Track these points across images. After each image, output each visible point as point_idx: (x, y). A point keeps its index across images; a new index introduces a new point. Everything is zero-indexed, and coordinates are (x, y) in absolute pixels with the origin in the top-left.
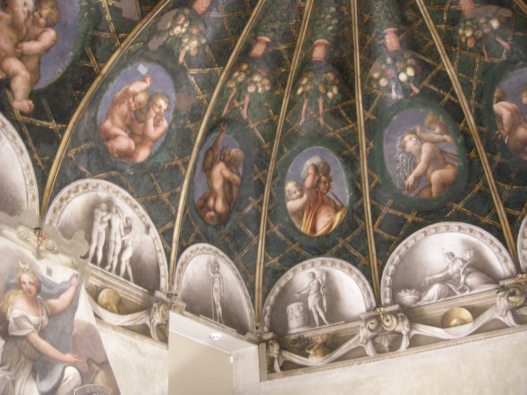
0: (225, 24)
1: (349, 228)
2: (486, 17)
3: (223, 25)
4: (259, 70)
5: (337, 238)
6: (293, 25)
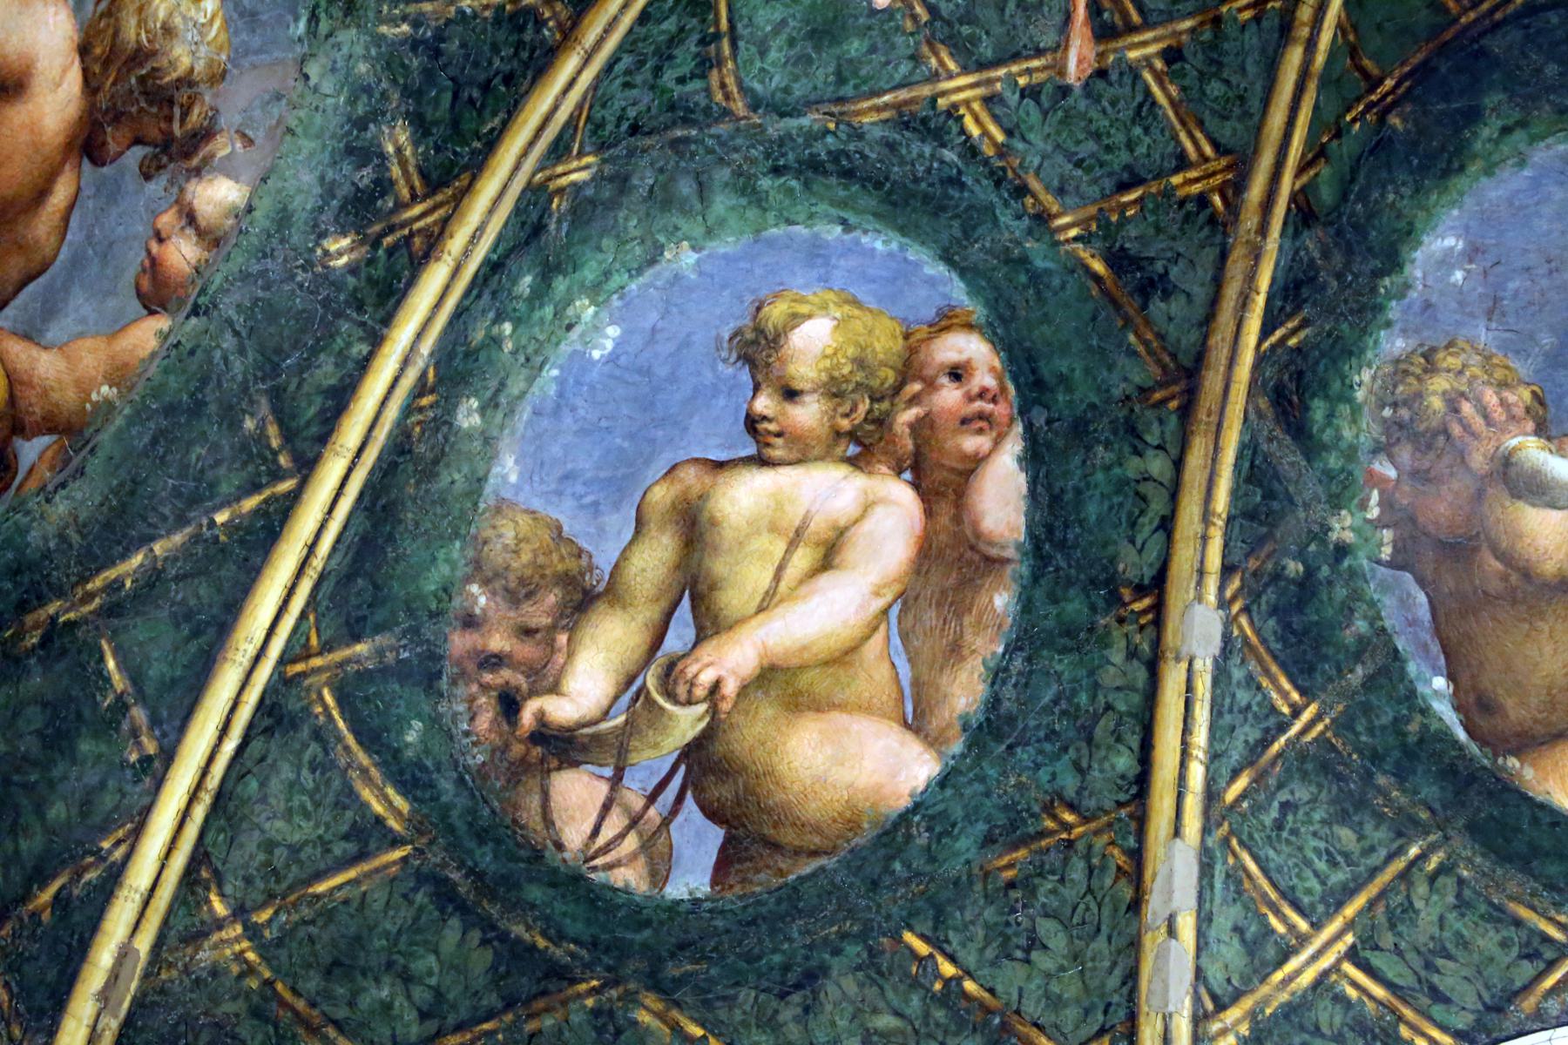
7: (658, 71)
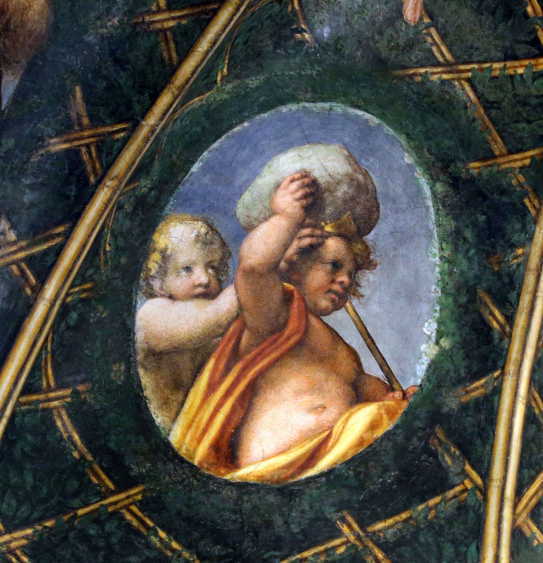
1: (399, 481)
5: (330, 512)
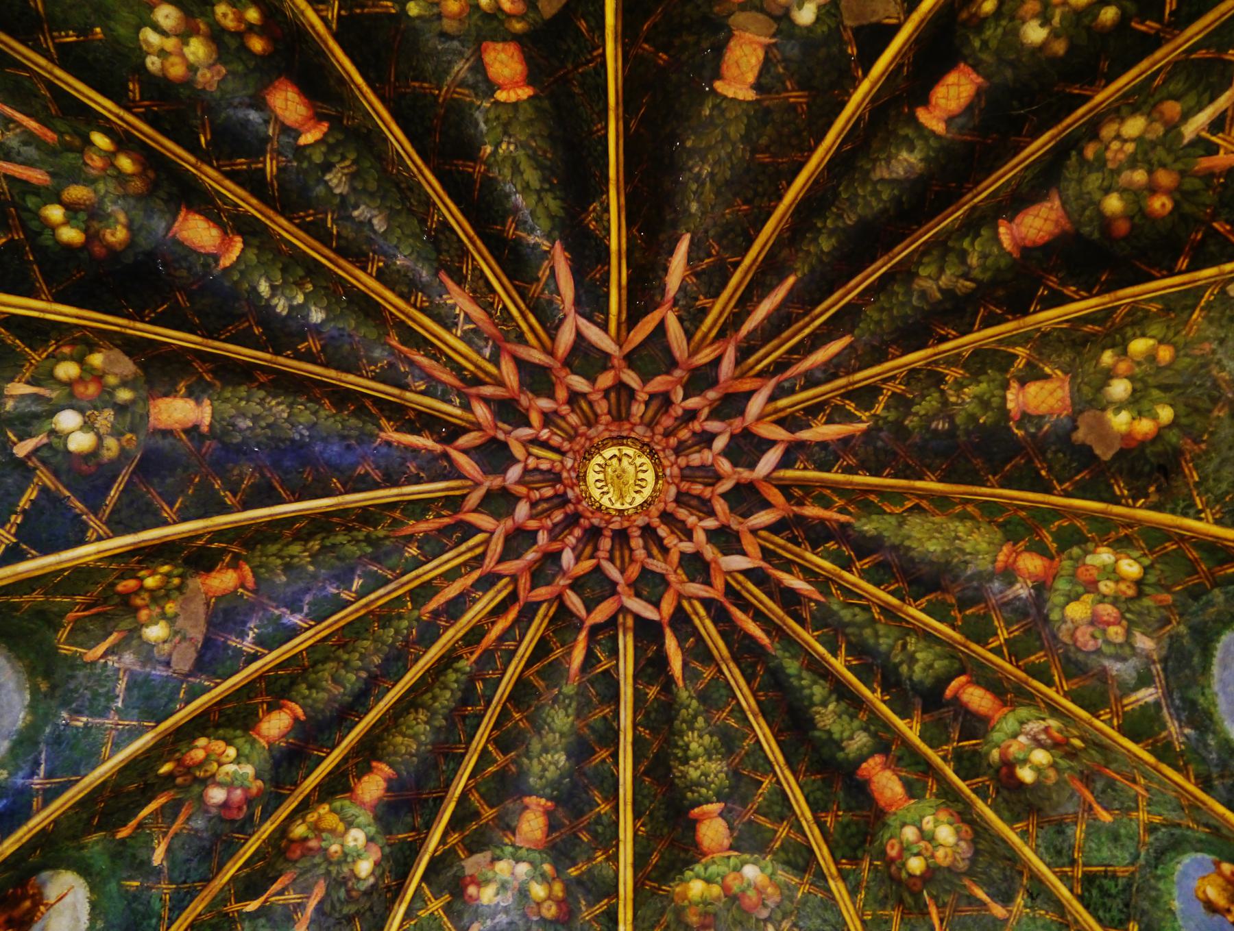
0: (426, 85)
2: (176, 615)
3: (424, 80)
4: (224, 71)
6: (324, 220)
7: (1110, 896)
